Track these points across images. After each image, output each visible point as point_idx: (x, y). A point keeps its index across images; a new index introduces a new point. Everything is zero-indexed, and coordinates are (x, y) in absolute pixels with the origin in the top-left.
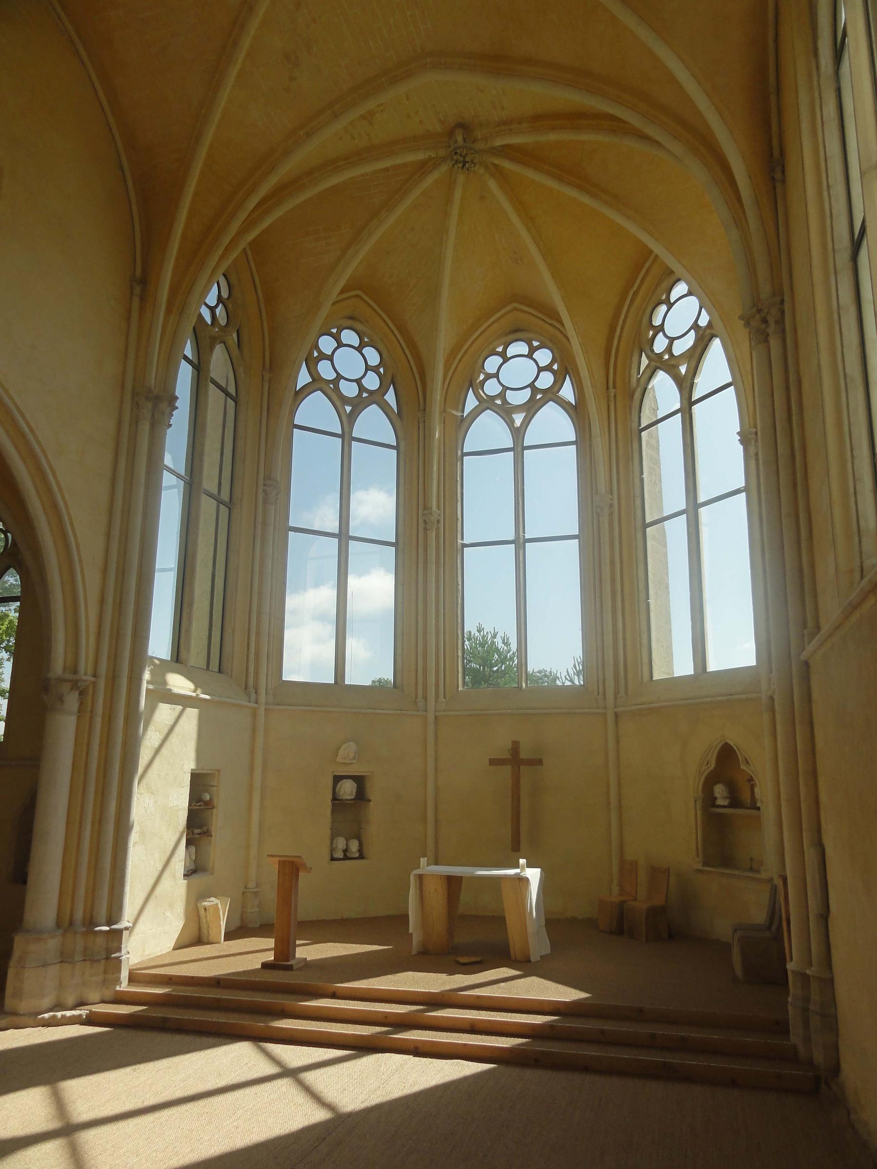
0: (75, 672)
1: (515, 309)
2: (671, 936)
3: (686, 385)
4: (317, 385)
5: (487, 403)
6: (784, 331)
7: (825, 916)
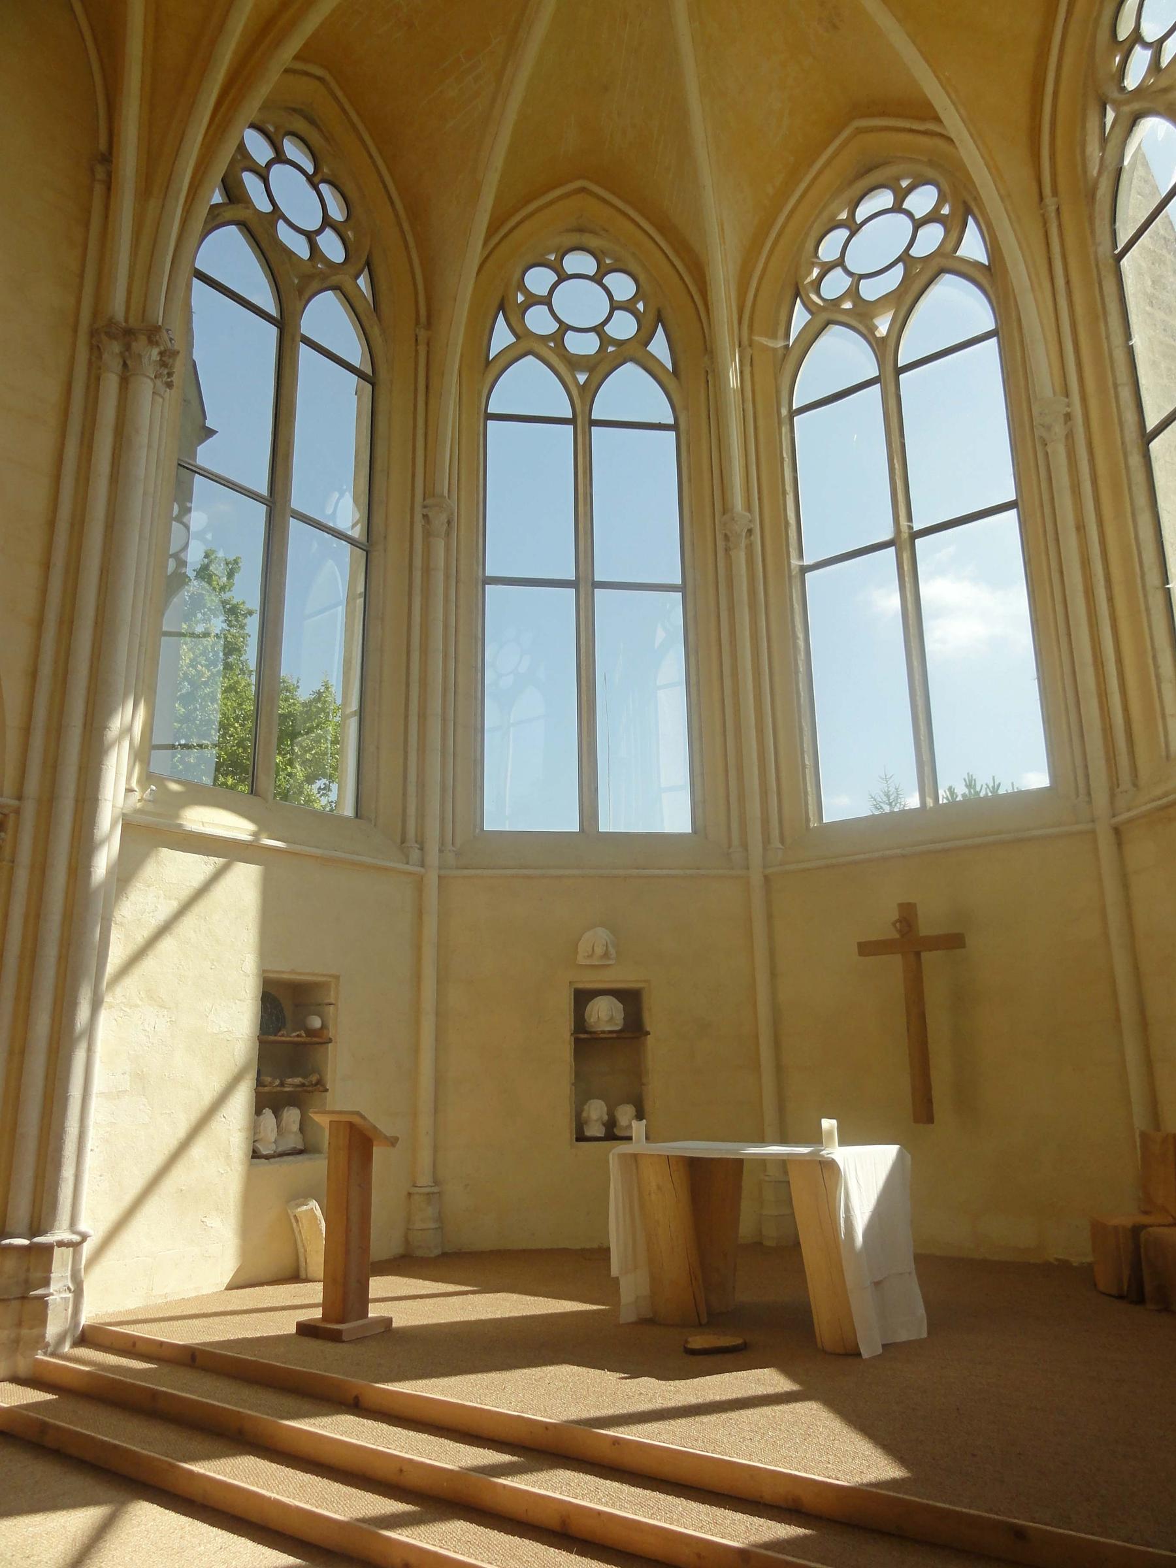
1: (859, 131)
4: (524, 345)
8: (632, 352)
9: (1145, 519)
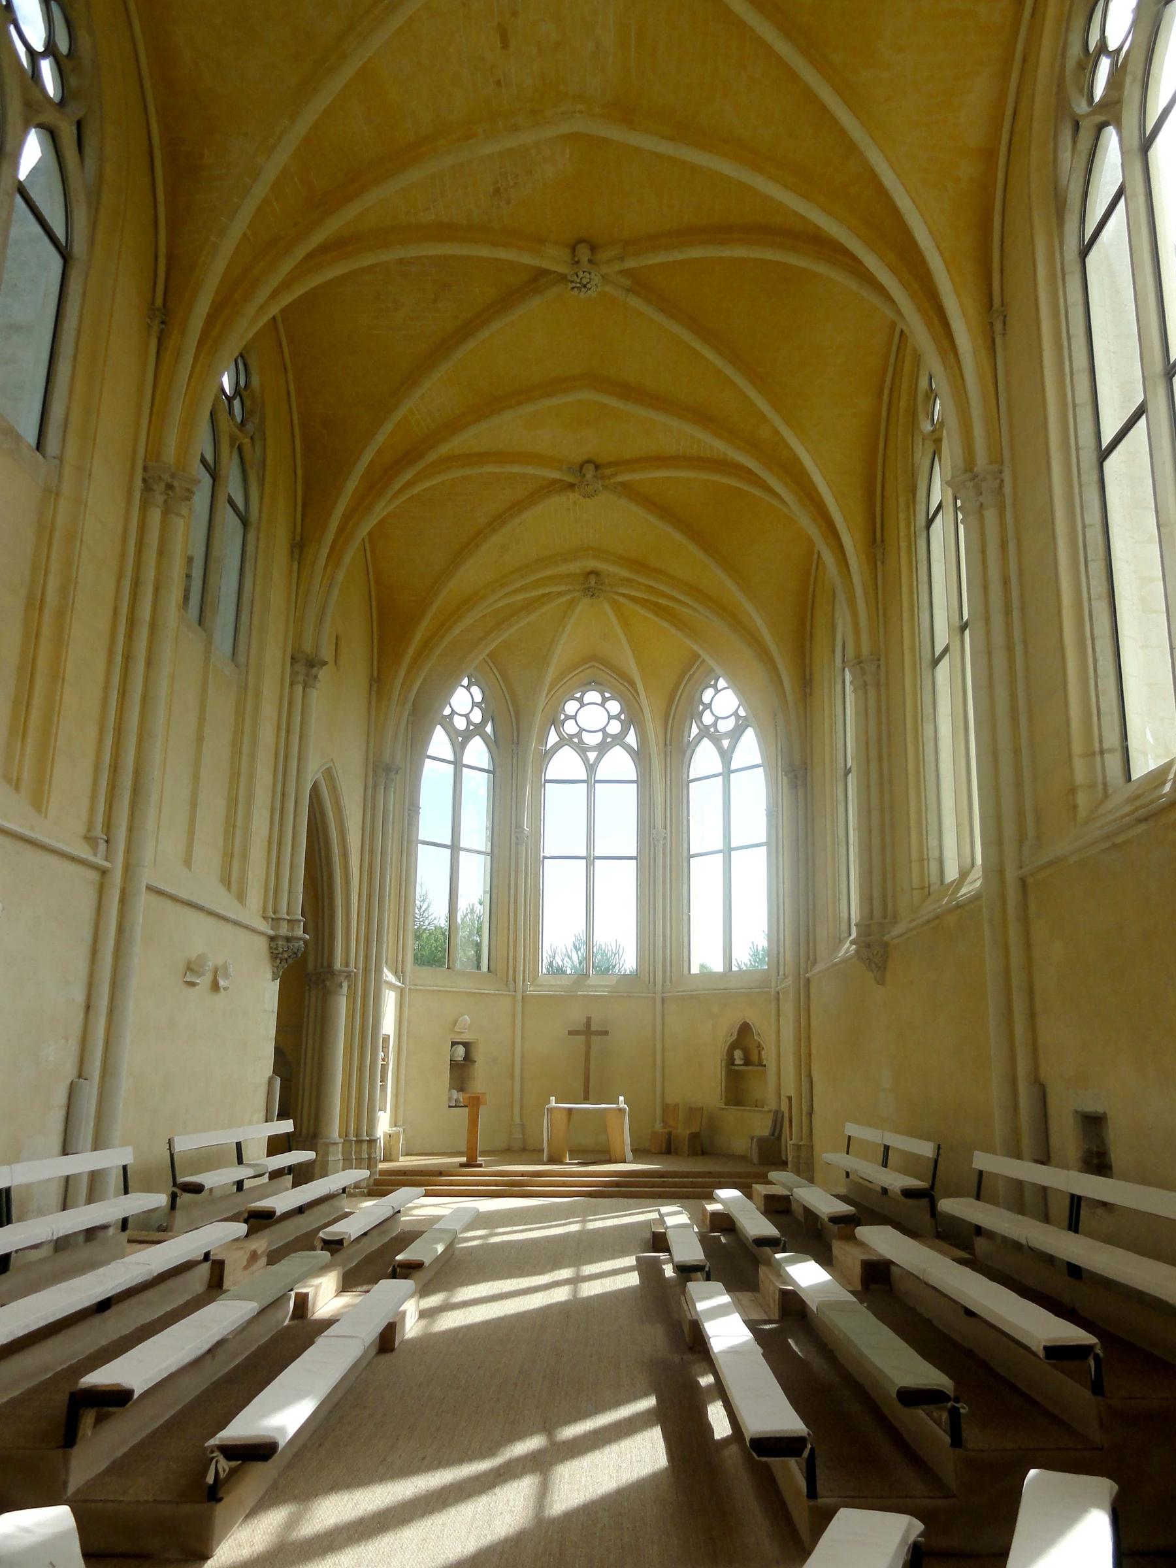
0: (347, 965)
2: (703, 1153)
3: (726, 756)
5: (565, 741)
6: (805, 786)
7: (810, 1114)
8: (478, 729)
9: (685, 886)
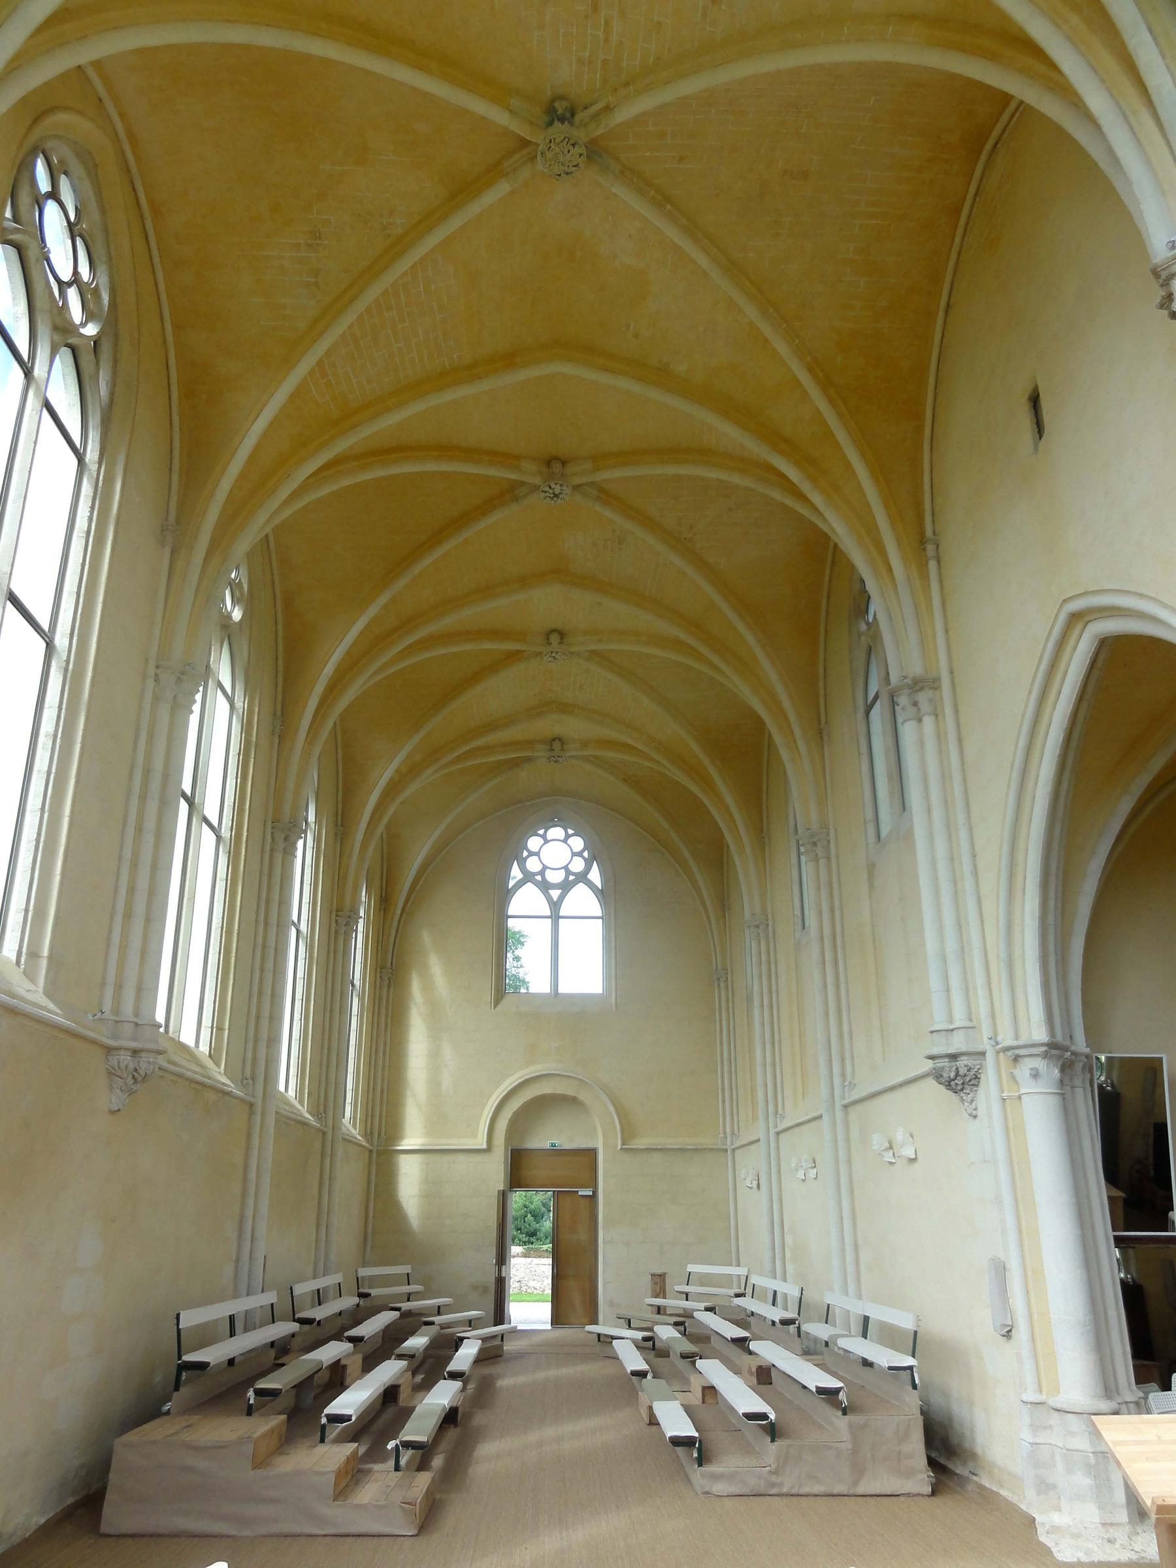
5: (528, 877)
